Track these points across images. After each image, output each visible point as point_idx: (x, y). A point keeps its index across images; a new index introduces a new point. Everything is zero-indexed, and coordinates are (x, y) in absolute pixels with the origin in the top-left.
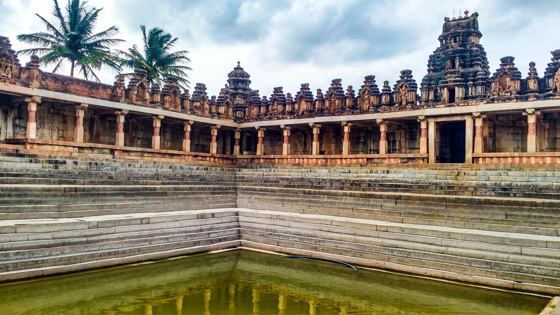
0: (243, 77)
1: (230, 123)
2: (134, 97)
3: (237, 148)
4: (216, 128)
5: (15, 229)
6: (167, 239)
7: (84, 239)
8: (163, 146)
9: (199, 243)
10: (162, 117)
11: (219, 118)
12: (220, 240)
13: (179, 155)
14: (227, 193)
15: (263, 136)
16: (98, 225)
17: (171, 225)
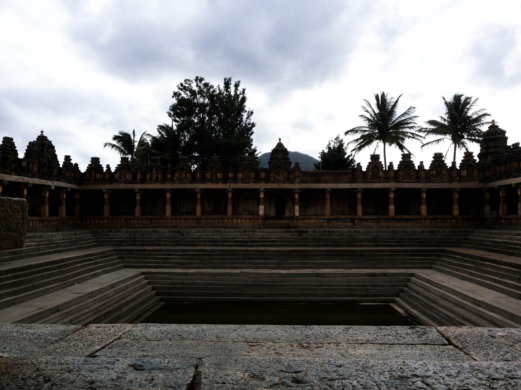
0: (495, 135)
1: (472, 185)
2: (369, 176)
3: (487, 208)
4: (456, 192)
5: (237, 274)
6: (329, 289)
7: (272, 284)
8: (397, 212)
9: (354, 295)
10: (393, 190)
11: (460, 181)
12: (376, 296)
13: (415, 219)
14: (430, 255)
15: (504, 195)
16: (286, 275)
17: (345, 279)
